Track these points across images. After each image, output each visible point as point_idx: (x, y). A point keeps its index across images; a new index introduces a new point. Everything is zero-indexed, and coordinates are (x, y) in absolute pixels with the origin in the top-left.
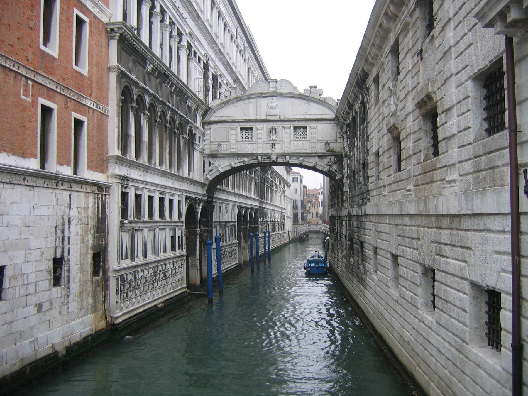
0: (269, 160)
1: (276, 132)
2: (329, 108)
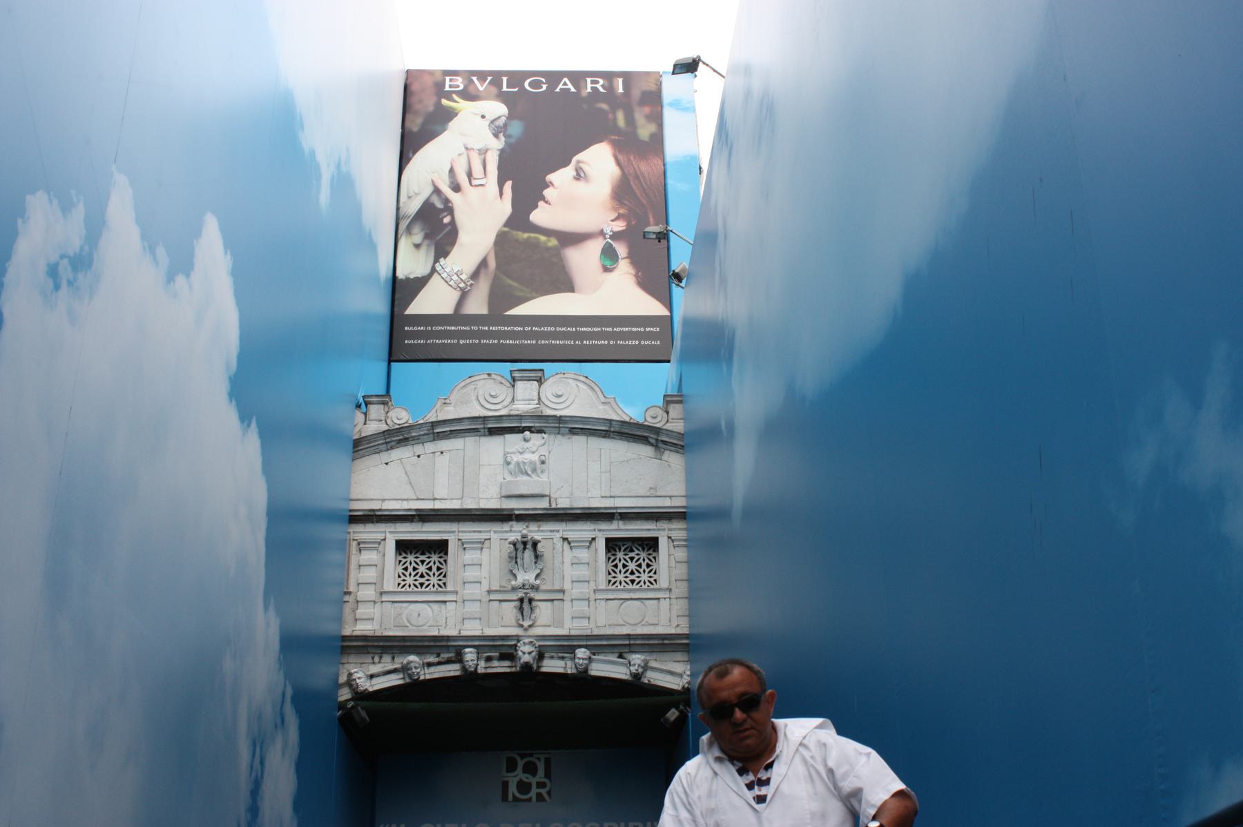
0: (507, 663)
1: (537, 557)
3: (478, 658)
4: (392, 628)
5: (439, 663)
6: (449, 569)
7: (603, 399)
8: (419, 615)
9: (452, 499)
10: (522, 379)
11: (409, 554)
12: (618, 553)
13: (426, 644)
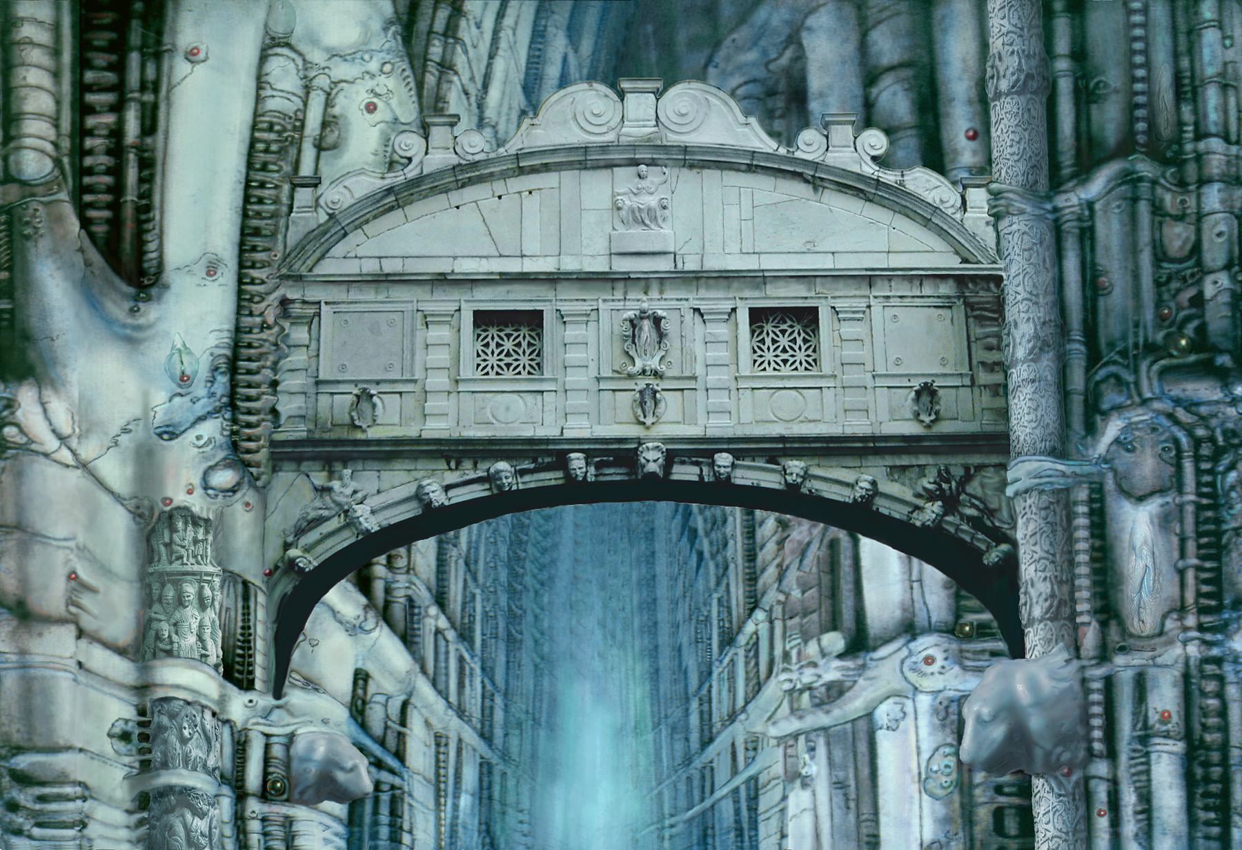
2: (926, 223)
3: (587, 464)
8: (508, 409)
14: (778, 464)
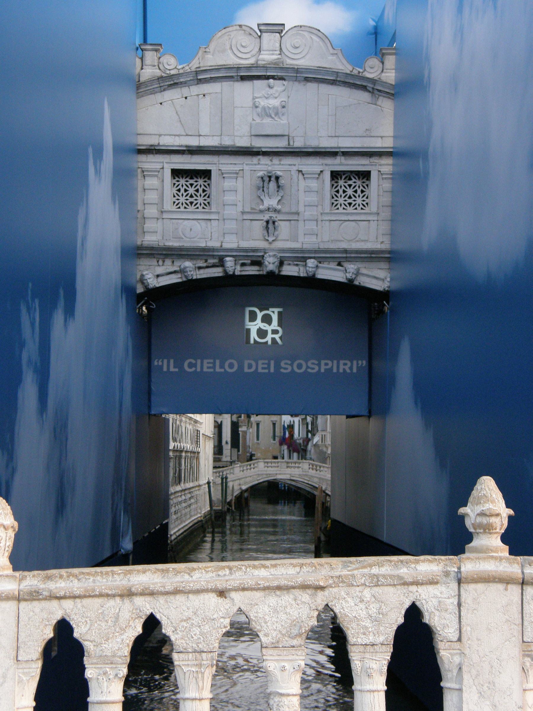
0: (256, 268)
1: (279, 187)
3: (235, 264)
4: (172, 239)
5: (207, 267)
6: (212, 191)
7: (332, 51)
8: (191, 229)
9: (213, 136)
10: (267, 31)
11: (181, 178)
12: (339, 181)
13: (198, 253)
14: (342, 266)
